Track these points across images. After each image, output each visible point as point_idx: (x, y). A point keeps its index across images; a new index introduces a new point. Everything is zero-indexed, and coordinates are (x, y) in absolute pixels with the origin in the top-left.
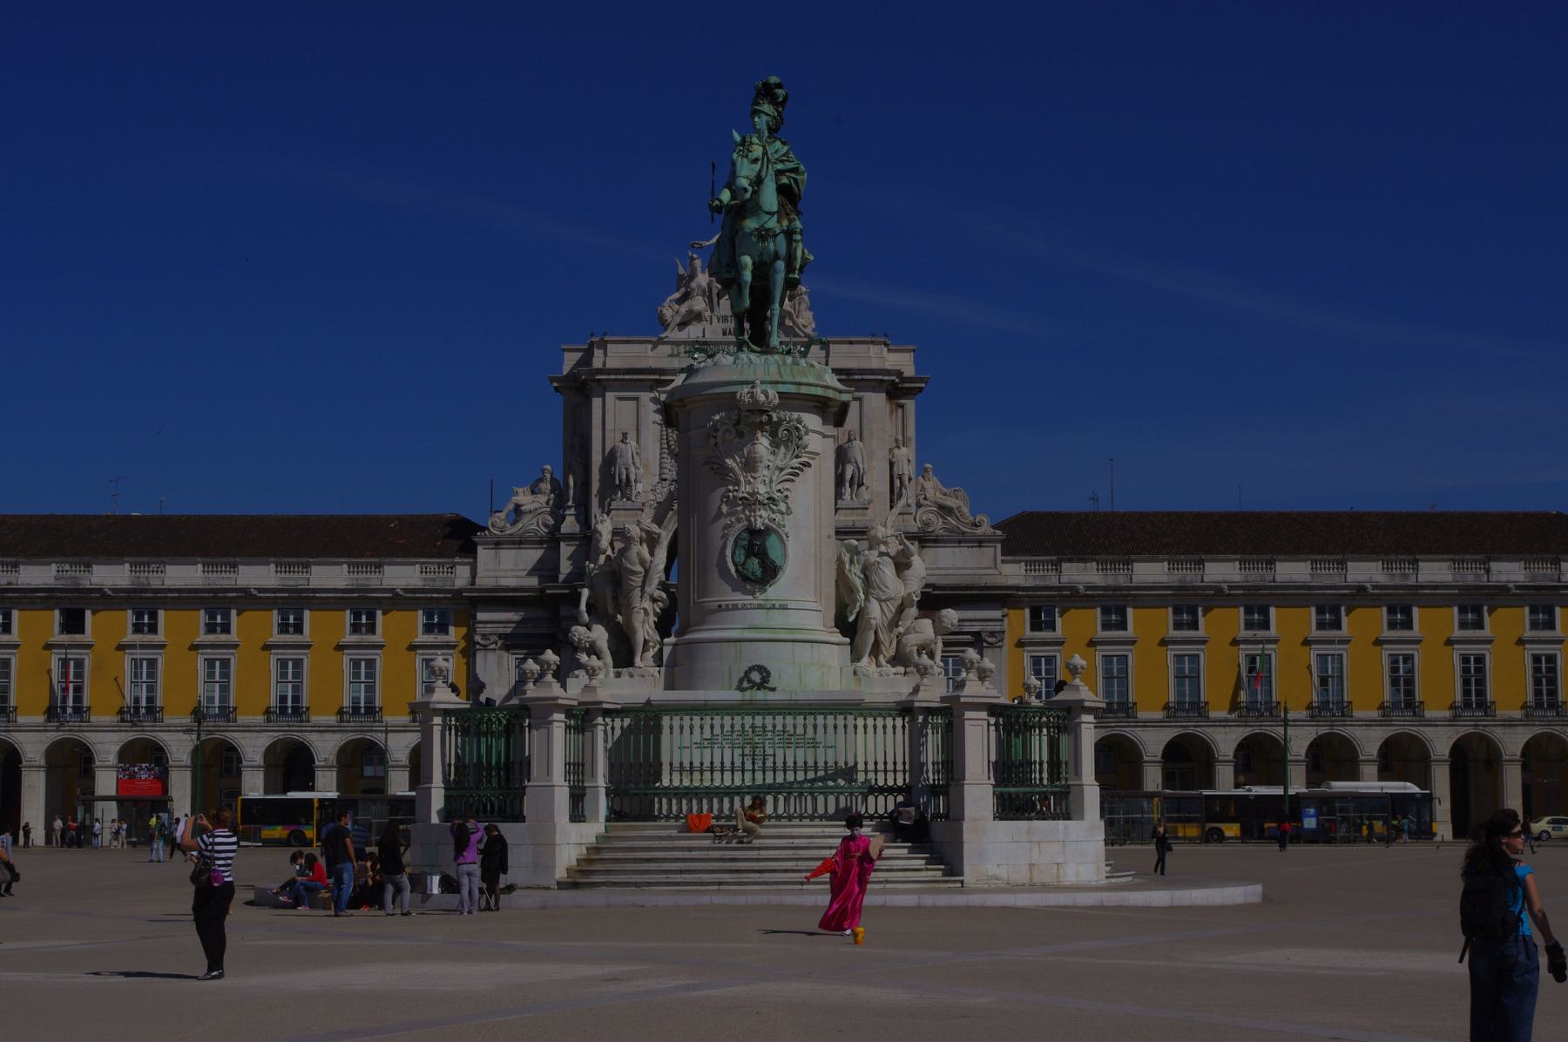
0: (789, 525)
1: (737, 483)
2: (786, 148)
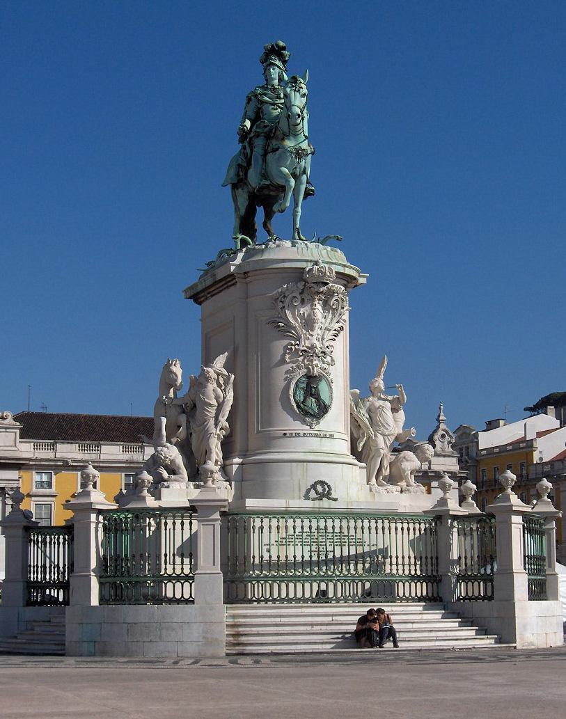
1: (299, 338)
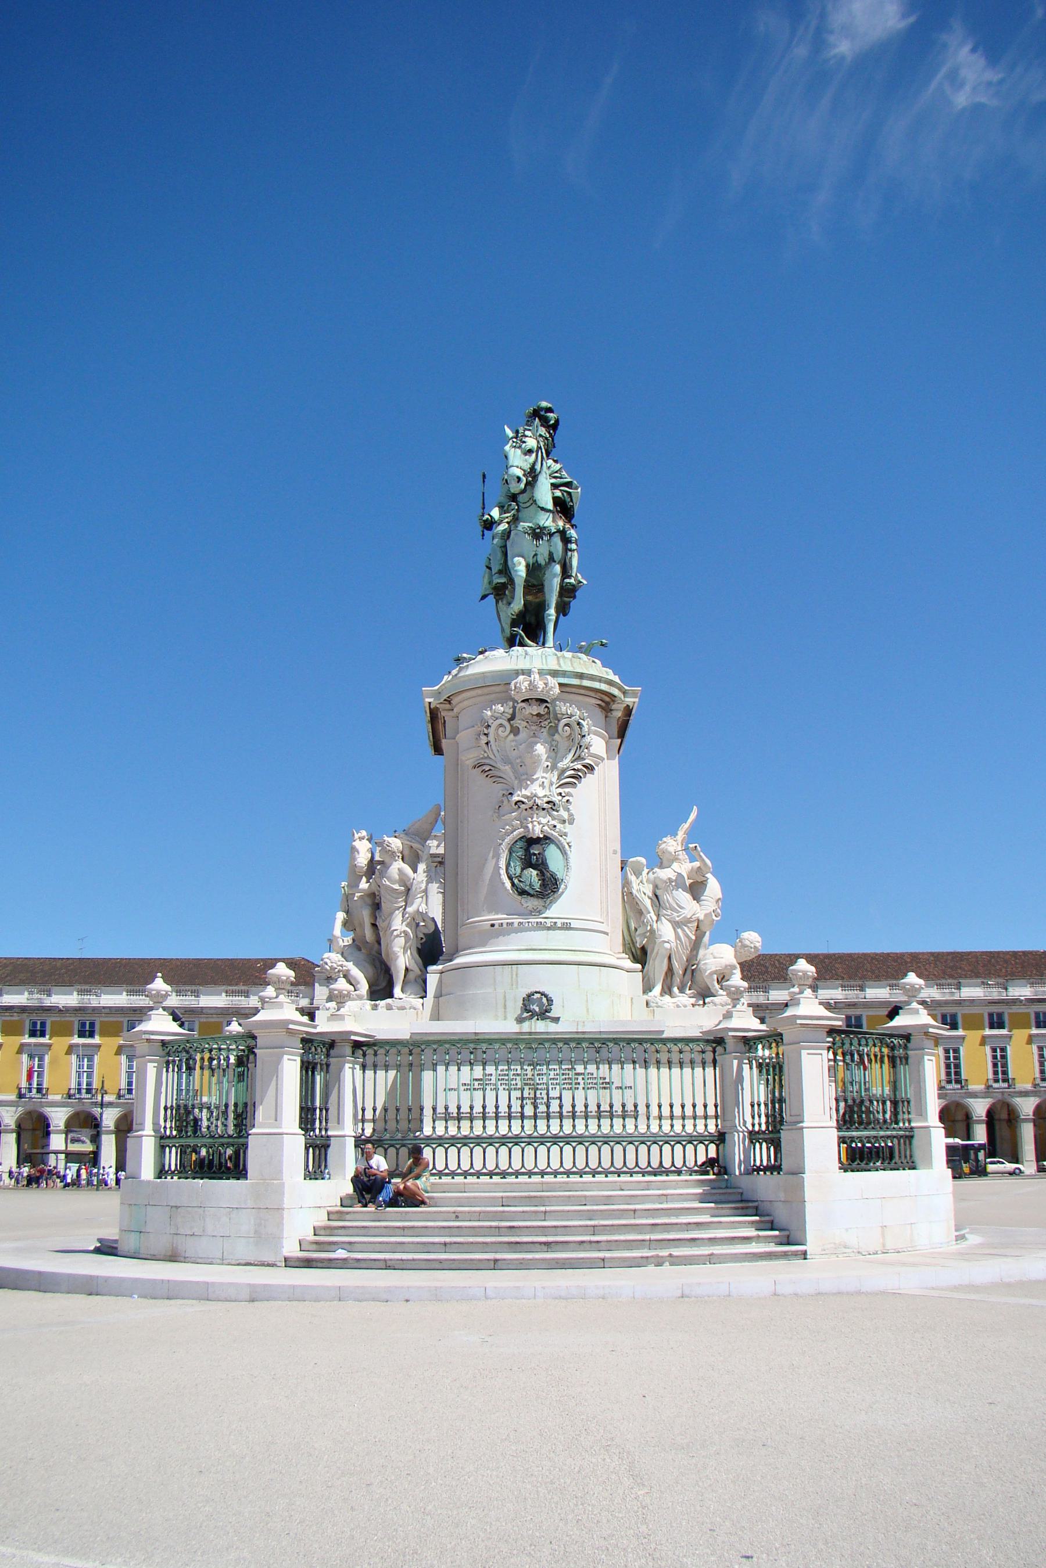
0: (572, 835)
2: (558, 466)
